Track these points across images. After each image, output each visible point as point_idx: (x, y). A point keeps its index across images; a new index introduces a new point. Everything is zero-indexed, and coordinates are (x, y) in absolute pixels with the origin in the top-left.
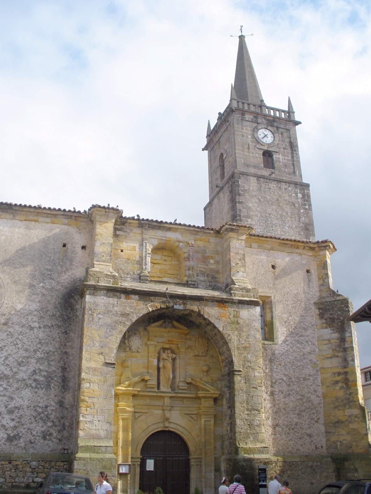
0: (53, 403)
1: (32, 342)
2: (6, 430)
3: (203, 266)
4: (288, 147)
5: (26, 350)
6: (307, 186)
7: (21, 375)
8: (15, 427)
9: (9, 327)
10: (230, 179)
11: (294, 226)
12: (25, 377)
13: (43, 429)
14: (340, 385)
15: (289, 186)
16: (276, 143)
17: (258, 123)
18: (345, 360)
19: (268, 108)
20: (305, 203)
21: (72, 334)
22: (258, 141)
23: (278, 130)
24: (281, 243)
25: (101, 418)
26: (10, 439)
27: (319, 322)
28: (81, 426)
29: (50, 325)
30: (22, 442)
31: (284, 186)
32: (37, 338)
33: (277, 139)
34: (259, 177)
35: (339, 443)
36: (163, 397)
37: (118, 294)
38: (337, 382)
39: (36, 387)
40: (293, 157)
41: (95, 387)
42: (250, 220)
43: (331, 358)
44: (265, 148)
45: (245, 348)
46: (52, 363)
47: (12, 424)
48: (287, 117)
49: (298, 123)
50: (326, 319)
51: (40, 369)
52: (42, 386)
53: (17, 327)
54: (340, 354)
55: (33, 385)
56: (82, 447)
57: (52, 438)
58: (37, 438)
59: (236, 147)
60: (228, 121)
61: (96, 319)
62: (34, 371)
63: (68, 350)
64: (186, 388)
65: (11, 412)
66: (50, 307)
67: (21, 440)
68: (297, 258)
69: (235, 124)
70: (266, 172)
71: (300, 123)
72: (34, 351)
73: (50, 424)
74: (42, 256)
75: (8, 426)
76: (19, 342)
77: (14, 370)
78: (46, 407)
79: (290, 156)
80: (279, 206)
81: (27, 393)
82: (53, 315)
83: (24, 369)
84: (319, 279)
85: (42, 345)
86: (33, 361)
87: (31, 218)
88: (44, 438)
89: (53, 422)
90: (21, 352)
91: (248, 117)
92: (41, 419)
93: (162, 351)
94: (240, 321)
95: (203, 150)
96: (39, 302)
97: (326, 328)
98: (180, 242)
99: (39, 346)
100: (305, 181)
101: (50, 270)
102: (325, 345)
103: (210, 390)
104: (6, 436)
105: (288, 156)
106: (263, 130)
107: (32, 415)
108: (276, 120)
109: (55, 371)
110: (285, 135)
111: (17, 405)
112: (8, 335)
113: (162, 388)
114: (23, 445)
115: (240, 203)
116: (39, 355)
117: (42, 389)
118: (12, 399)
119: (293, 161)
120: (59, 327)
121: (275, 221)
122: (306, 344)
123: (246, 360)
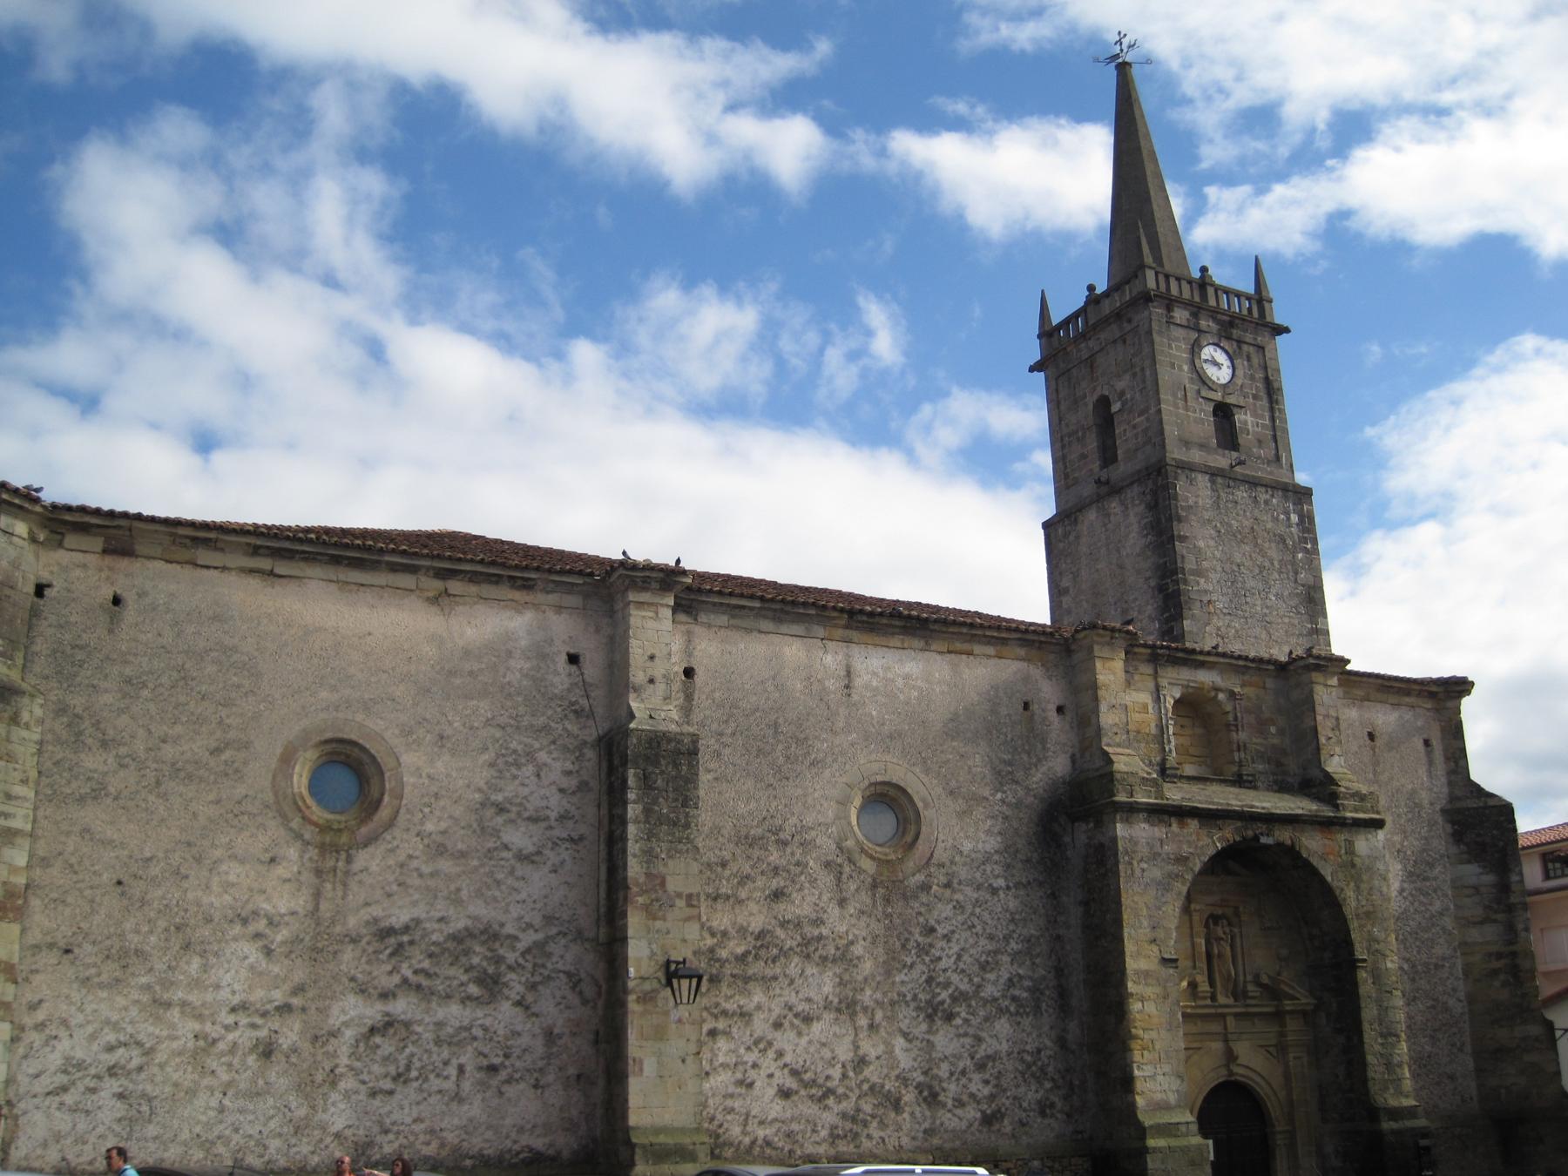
0: (1048, 1043)
1: (999, 919)
2: (978, 1103)
3: (1259, 741)
4: (1263, 394)
5: (991, 937)
7: (989, 991)
8: (992, 1097)
9: (954, 891)
10: (1149, 475)
11: (1286, 593)
12: (997, 994)
13: (1039, 1096)
14: (1502, 977)
15: (1273, 496)
16: (1239, 382)
17: (1200, 331)
18: (1511, 928)
19: (1217, 289)
20: (1306, 535)
21: (1064, 899)
22: (1203, 380)
23: (1240, 348)
24: (1383, 686)
25: (1167, 1068)
26: (988, 1120)
27: (1454, 850)
28: (1139, 1086)
29: (1024, 880)
30: (1007, 1126)
31: (1263, 496)
32: (1007, 911)
33: (1240, 372)
34: (1214, 474)
35: (1503, 1091)
36: (1223, 1016)
37: (1166, 818)
38: (1494, 973)
39: (1017, 1013)
40: (1273, 419)
41: (1151, 1008)
42: (1202, 581)
43: (1482, 923)
44: (1218, 396)
45: (1368, 914)
46: (1038, 961)
47: (986, 1091)
48: (1245, 312)
49: (1282, 330)
51: (1019, 975)
52: (1028, 1010)
53: (968, 891)
54: (1500, 917)
55: (1012, 1009)
56: (1151, 1127)
57: (1055, 1111)
58: (1032, 1114)
59: (1162, 396)
60: (1129, 321)
61: (1138, 872)
62: (1010, 980)
63: (1062, 932)
64: (1258, 994)
65: (981, 1067)
67: (1006, 1122)
68: (1408, 715)
69: (1155, 335)
70: (1222, 460)
71: (1287, 330)
72: (1004, 938)
73: (1048, 1085)
74: (991, 733)
75: (980, 1095)
76: (976, 921)
77: (976, 980)
78: (1039, 1051)
79: (1267, 415)
80: (1256, 545)
81: (1003, 1026)
82: (1028, 861)
83: (991, 976)
84: (1447, 759)
85: (1016, 924)
86: (1006, 959)
87: (959, 646)
88: (1043, 1113)
89: (1053, 1080)
90: (983, 942)
91: (1180, 315)
92: (1033, 1075)
93: (1211, 921)
94: (1357, 861)
95: (1032, 369)
96: (1000, 833)
97: (1469, 862)
98: (1217, 690)
99: (1011, 927)
100: (1302, 478)
101: (1010, 763)
102: (1468, 896)
103: (1298, 996)
104: (979, 1115)
105: (1262, 417)
106: (1211, 348)
107: (1017, 1069)
108: (1237, 321)
109: (1044, 978)
110: (1255, 361)
111: (990, 1052)
112: (955, 907)
113: (1222, 1000)
114: (1008, 1129)
115: (1183, 539)
116: (1014, 945)
117: (1028, 1015)
118: (979, 1040)
119: (1274, 428)
120: (1041, 884)
121: (1251, 583)
122: (1434, 895)
123: (1372, 940)
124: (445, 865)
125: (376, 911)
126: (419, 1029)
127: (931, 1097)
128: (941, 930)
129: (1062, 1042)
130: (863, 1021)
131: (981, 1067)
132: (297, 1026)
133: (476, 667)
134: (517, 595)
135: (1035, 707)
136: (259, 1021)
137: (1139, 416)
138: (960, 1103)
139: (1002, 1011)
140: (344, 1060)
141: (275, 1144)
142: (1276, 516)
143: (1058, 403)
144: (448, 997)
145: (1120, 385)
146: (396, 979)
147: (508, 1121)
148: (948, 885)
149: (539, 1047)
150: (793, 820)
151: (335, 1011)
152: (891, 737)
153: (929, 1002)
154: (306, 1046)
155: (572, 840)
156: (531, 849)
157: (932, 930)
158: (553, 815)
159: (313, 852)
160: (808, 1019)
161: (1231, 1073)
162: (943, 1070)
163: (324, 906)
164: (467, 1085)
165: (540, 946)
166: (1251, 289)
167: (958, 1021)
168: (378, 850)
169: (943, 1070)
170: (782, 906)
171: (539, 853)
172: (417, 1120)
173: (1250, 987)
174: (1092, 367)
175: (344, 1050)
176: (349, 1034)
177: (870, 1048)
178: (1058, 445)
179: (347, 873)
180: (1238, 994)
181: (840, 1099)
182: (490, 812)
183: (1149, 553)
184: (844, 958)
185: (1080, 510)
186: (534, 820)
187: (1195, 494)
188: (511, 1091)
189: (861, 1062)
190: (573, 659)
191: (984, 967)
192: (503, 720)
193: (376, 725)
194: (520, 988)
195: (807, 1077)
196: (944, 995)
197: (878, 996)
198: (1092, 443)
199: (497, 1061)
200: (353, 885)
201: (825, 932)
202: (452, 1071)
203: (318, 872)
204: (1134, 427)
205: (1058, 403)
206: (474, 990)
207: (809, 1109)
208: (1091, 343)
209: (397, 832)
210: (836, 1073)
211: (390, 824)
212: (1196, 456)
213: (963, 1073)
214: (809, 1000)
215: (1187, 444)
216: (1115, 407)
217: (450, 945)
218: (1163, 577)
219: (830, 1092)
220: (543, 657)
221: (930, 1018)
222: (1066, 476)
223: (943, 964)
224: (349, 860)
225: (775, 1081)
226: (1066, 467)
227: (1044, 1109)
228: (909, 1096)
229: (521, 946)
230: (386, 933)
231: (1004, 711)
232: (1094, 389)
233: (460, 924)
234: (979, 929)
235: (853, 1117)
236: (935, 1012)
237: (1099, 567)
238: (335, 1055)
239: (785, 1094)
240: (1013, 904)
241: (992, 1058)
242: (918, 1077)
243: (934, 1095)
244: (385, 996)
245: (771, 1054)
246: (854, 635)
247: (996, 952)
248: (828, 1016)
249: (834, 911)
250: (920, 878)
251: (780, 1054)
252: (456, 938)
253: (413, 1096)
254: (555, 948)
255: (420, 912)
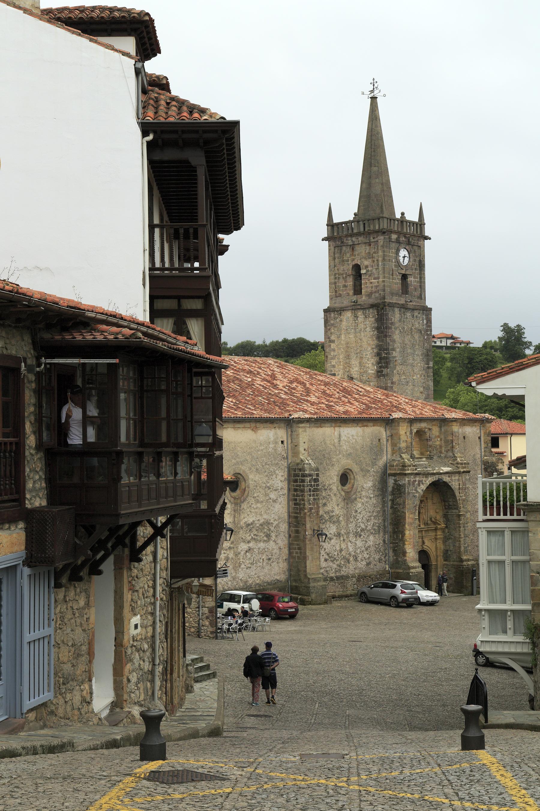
6: (430, 309)
7: (369, 527)
8: (369, 558)
26: (368, 564)
28: (407, 555)
30: (372, 566)
40: (421, 278)
44: (403, 272)
47: (368, 556)
50: (488, 472)
66: (377, 483)
71: (430, 239)
81: (371, 538)
82: (378, 488)
83: (369, 523)
86: (373, 518)
88: (380, 562)
90: (368, 513)
95: (323, 240)
105: (417, 278)
116: (375, 514)
118: (366, 542)
119: (421, 282)
120: (381, 495)
124: (259, 505)
125: (246, 520)
126: (255, 550)
127: (356, 559)
128: (359, 511)
129: (384, 541)
130: (342, 539)
131: (367, 549)
132: (232, 552)
133: (263, 448)
134: (270, 425)
135: (381, 441)
136: (225, 552)
137: (374, 279)
138: (362, 560)
139: (372, 533)
140: (241, 560)
141: (230, 583)
142: (419, 323)
143: (334, 259)
144: (261, 541)
145: (366, 263)
146: (250, 537)
147: (273, 573)
148: (360, 498)
149: (278, 551)
150: (328, 482)
151: (239, 547)
152: (349, 455)
153: (356, 532)
154: (234, 557)
155: (283, 495)
156: (275, 498)
157: (357, 511)
158: (279, 488)
159: (233, 505)
160: (330, 539)
161: (423, 548)
162: (358, 551)
163: (236, 519)
164: (264, 564)
165: (277, 525)
166: (416, 219)
167: (362, 537)
168: (245, 503)
169: (358, 551)
170: (325, 508)
171: (277, 499)
172: (255, 574)
173: (429, 522)
174: (353, 249)
175: (241, 557)
176: (242, 553)
177: (343, 546)
178: (333, 277)
179: (240, 510)
180: (426, 524)
181: (337, 560)
182: (267, 489)
183: (375, 339)
184: (338, 521)
185: (343, 310)
186: (276, 490)
187: (395, 316)
188: (273, 564)
189: (341, 550)
190: (282, 442)
191: (368, 521)
192: (269, 463)
193: (243, 468)
194: (274, 537)
195: (330, 555)
196: (359, 530)
197: (345, 531)
198: (350, 282)
199: (270, 557)
200: (241, 514)
201: (334, 514)
202: (262, 561)
203: (235, 511)
204: (371, 283)
205: (334, 259)
206: (265, 538)
207: (331, 564)
208: (354, 239)
209: (249, 498)
210: (336, 553)
211: (247, 496)
212: (394, 300)
213: (363, 551)
214: (331, 534)
215: (392, 294)
216: (363, 271)
217: (260, 527)
218: (380, 350)
219: (335, 559)
220: (276, 443)
221: (356, 536)
222: (336, 291)
223: (359, 521)
224: (240, 507)
225: (324, 557)
226: (336, 288)
227: (380, 560)
228: (351, 559)
229: (274, 525)
230: (248, 525)
231: (374, 443)
232: (353, 260)
233: (262, 521)
234: (367, 510)
235: (339, 566)
236: (357, 535)
237: (351, 337)
238: (239, 559)
239: (326, 560)
240: (375, 502)
241: (369, 547)
242: (353, 553)
243: (356, 558)
244: (249, 542)
245: (323, 550)
246: (342, 425)
247: (370, 516)
248: (335, 538)
249: (336, 508)
250: (354, 496)
251: (325, 549)
252: (261, 525)
253: (255, 568)
254: (281, 525)
255: (254, 519)
